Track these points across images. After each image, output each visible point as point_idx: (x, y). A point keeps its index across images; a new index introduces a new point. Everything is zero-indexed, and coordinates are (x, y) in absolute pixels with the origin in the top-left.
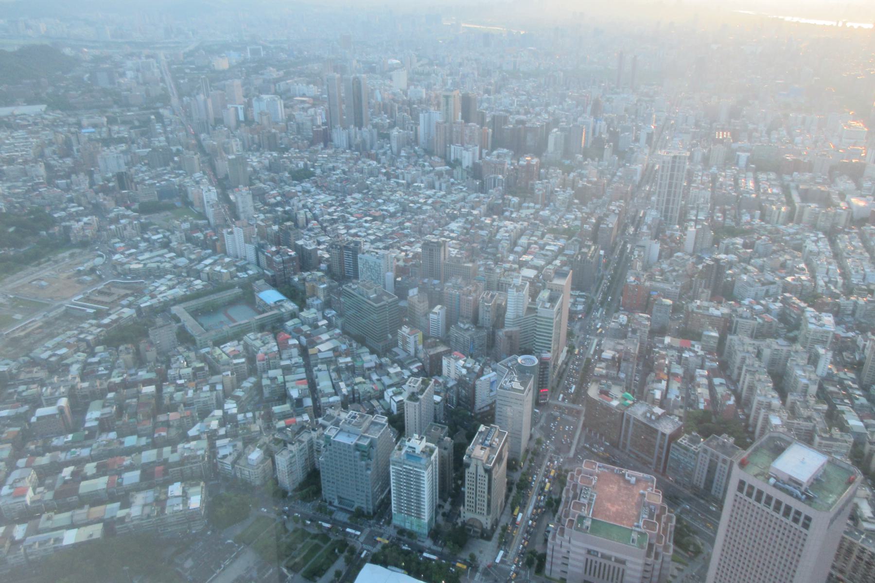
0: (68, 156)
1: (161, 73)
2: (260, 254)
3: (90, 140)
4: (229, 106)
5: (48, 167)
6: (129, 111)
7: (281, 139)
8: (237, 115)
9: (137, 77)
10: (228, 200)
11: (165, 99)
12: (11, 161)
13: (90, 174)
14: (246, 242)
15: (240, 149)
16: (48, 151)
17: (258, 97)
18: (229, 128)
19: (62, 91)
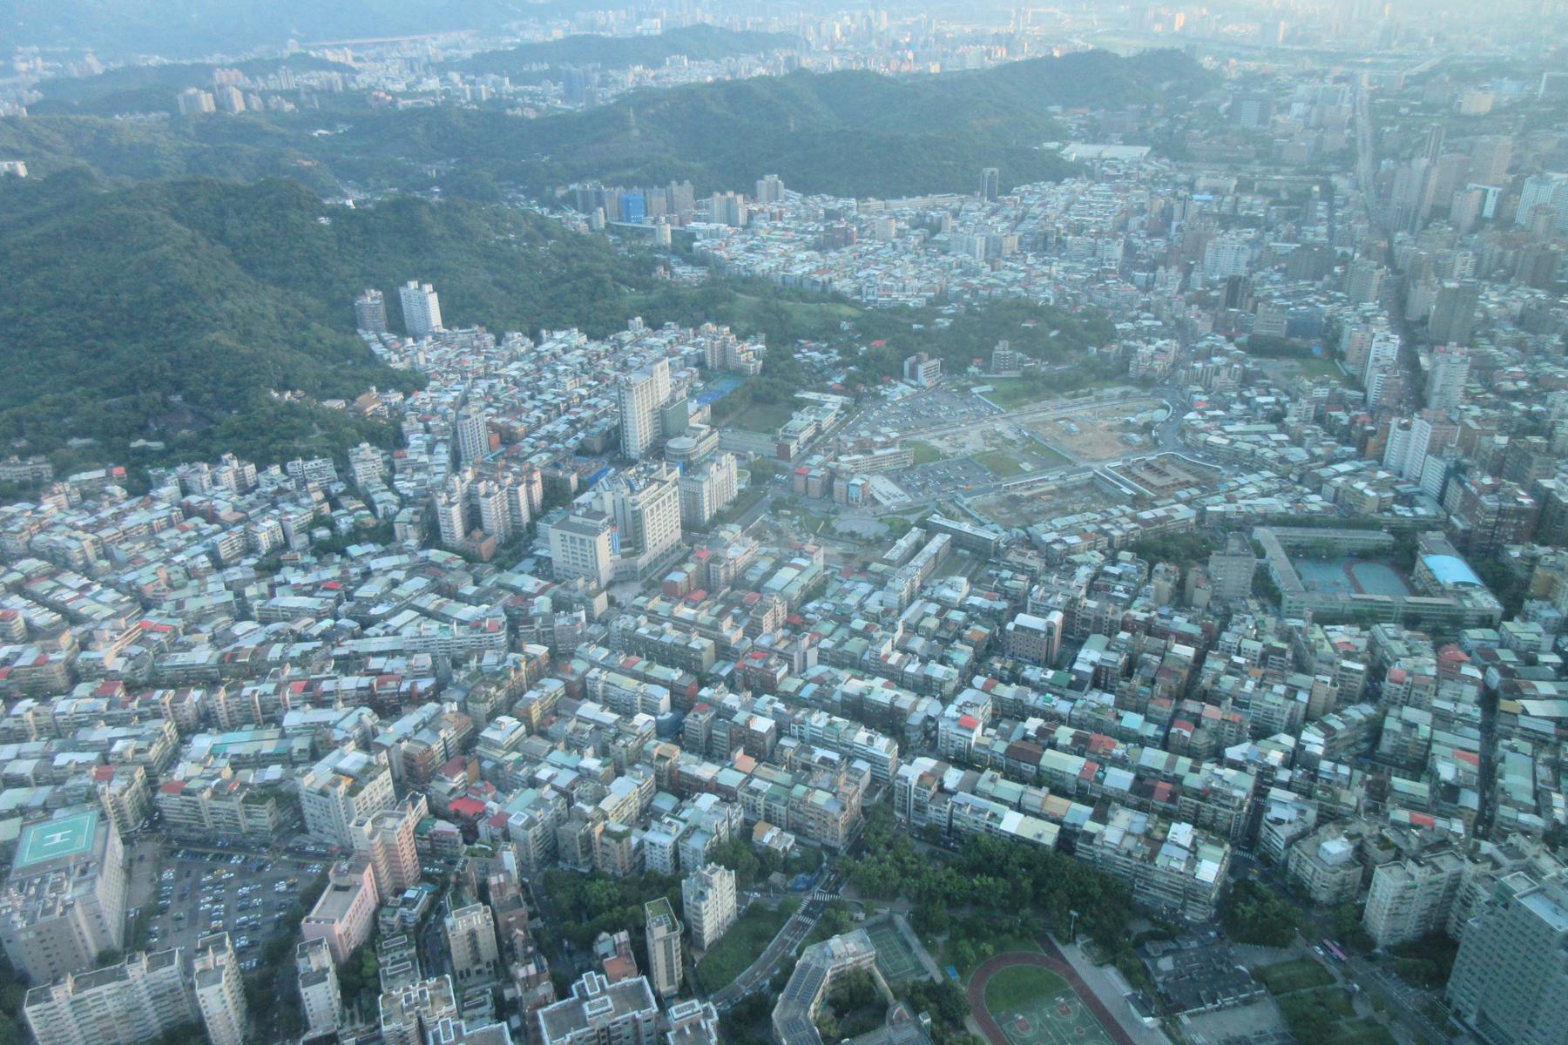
0: (1160, 234)
1: (1354, 110)
2: (1452, 483)
3: (1202, 214)
4: (1471, 185)
5: (1129, 249)
6: (1277, 172)
7: (1564, 266)
8: (1482, 207)
9: (1308, 115)
10: (1414, 365)
11: (1346, 159)
12: (1078, 229)
13: (1187, 271)
14: (1430, 452)
15: (1469, 270)
16: (1133, 222)
17: (1540, 174)
18: (1457, 228)
19: (1180, 127)
